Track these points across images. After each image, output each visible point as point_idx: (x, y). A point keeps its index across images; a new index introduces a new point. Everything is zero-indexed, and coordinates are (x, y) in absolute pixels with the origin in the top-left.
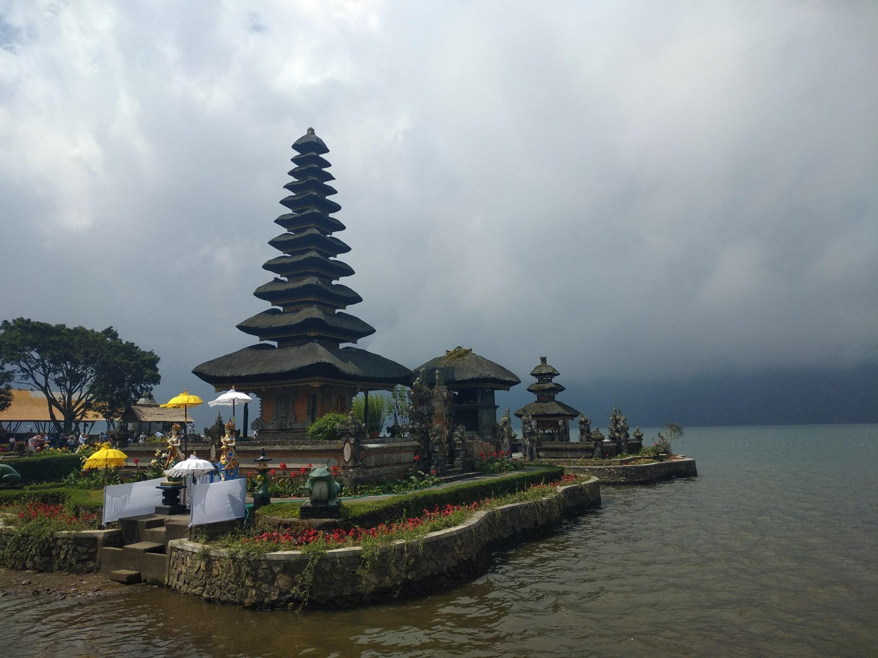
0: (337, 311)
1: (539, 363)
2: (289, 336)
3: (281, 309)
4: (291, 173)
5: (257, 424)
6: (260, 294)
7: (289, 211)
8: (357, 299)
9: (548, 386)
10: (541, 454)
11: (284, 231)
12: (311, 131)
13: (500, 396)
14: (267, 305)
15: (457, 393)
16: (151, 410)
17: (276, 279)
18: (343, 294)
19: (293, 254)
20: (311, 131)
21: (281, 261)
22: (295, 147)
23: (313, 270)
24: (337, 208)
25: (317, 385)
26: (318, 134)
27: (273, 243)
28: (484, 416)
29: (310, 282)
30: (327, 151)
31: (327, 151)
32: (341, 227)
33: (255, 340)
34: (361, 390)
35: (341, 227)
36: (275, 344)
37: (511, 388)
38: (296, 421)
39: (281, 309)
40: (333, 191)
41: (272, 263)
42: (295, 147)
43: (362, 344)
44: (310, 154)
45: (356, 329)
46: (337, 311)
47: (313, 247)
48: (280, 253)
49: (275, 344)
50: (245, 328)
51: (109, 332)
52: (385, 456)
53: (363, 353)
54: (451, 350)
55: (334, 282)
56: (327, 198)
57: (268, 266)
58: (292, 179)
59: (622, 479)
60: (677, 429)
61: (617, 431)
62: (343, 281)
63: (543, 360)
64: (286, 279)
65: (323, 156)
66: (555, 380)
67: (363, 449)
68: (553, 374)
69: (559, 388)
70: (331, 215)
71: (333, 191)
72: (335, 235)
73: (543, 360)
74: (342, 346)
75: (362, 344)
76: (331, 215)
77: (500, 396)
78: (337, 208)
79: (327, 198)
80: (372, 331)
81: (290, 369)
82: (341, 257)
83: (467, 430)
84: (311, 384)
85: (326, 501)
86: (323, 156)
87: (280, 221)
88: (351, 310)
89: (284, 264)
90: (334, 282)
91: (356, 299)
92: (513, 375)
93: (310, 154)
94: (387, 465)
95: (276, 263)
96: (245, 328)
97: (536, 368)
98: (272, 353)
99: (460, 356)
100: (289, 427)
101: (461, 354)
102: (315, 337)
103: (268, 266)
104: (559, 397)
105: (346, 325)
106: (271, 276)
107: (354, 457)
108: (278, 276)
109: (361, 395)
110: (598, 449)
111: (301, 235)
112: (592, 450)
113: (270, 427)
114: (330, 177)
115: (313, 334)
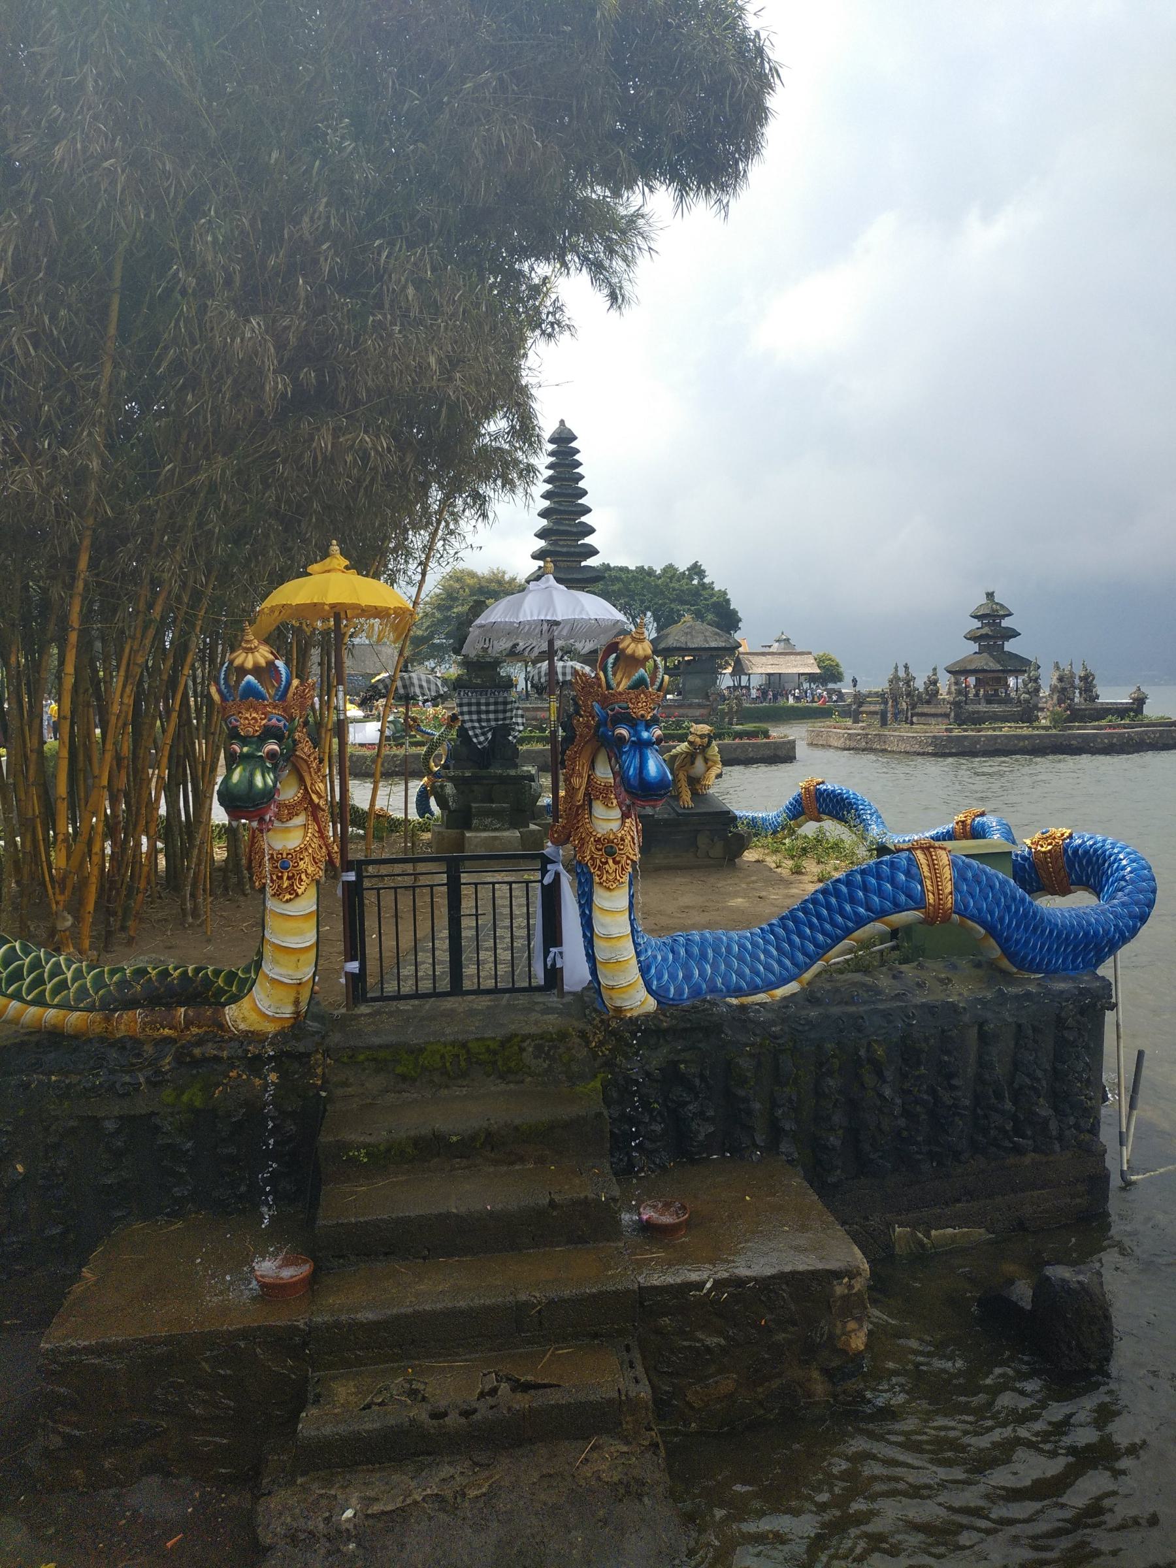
10: (915, 719)
12: (562, 422)
16: (763, 659)
20: (562, 422)
26: (568, 425)
30: (575, 438)
31: (575, 438)
51: (696, 570)
55: (583, 564)
59: (930, 749)
61: (1028, 693)
63: (990, 595)
69: (1013, 634)
70: (580, 501)
73: (990, 595)
76: (580, 501)
82: (588, 540)
86: (573, 445)
90: (583, 564)
104: (1010, 646)
110: (952, 714)
112: (947, 715)
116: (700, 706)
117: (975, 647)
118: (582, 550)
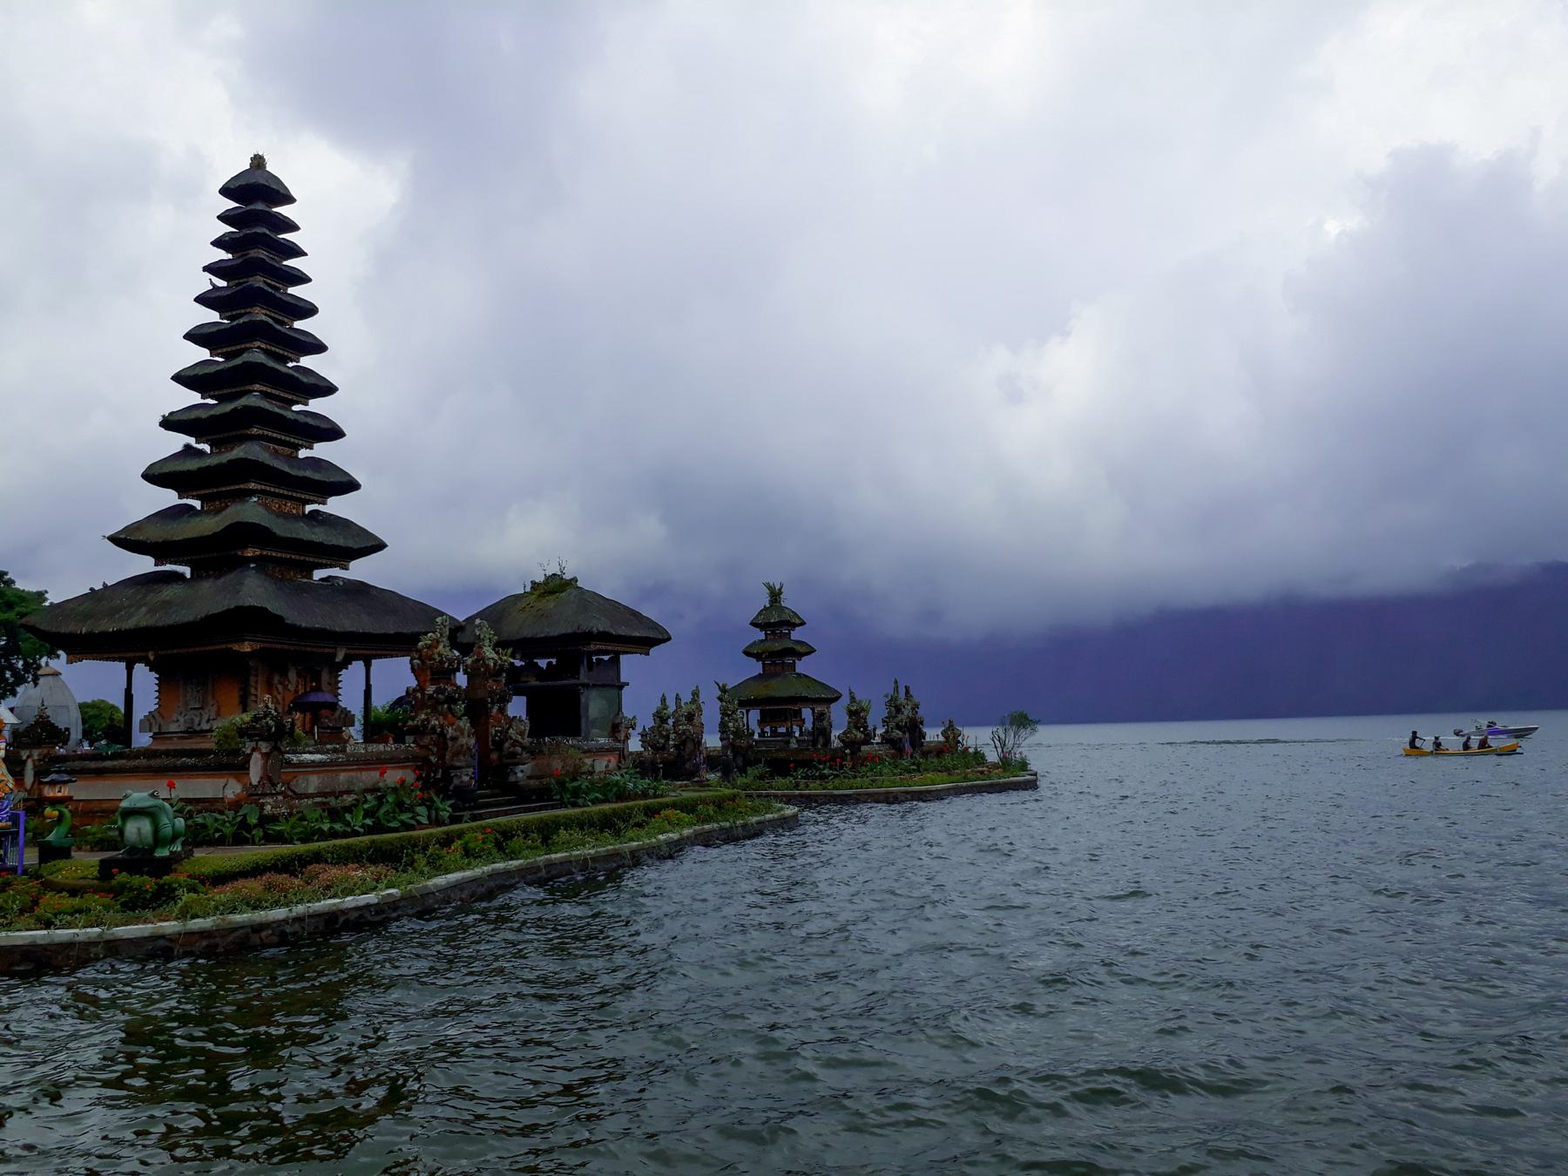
0: (308, 508)
1: (765, 601)
2: (213, 555)
3: (197, 504)
4: (217, 243)
5: (148, 722)
6: (156, 476)
7: (213, 316)
8: (348, 485)
9: (778, 646)
11: (203, 354)
12: (258, 162)
13: (631, 665)
14: (168, 498)
15: (554, 661)
17: (188, 447)
18: (317, 477)
19: (221, 399)
20: (258, 162)
21: (193, 415)
22: (226, 191)
23: (255, 431)
24: (309, 310)
25: (247, 648)
26: (270, 167)
27: (178, 378)
28: (594, 705)
29: (242, 455)
30: (288, 199)
31: (288, 199)
32: (318, 347)
33: (144, 564)
34: (357, 658)
35: (318, 347)
36: (187, 571)
37: (653, 651)
38: (218, 714)
39: (197, 504)
40: (302, 279)
41: (176, 418)
42: (226, 191)
43: (360, 570)
44: (256, 204)
45: (341, 542)
46: (308, 508)
47: (257, 387)
48: (195, 398)
49: (187, 571)
50: (126, 540)
52: (343, 777)
53: (360, 590)
54: (540, 579)
55: (303, 453)
56: (291, 290)
57: (169, 423)
58: (223, 255)
60: (1022, 721)
62: (321, 450)
63: (775, 595)
64: (206, 448)
65: (283, 210)
66: (796, 634)
67: (289, 763)
68: (792, 623)
70: (298, 325)
71: (302, 279)
72: (307, 361)
73: (775, 595)
74: (318, 574)
75: (360, 570)
76: (298, 325)
77: (631, 665)
78: (309, 310)
79: (291, 290)
80: (380, 546)
81: (191, 618)
82: (316, 405)
83: (575, 731)
84: (236, 647)
85: (152, 849)
86: (283, 210)
87: (196, 336)
88: (336, 506)
89: (198, 420)
90: (303, 453)
91: (348, 485)
92: (655, 626)
93: (256, 204)
94: (349, 792)
95: (184, 417)
96: (126, 540)
97: (760, 613)
98: (170, 592)
99: (552, 592)
100: (205, 727)
101: (555, 586)
102: (251, 559)
103: (169, 423)
104: (802, 666)
105: (318, 535)
106: (177, 441)
107: (268, 778)
108: (192, 441)
109: (357, 667)
111: (238, 361)
113: (173, 728)
114: (297, 252)
115: (249, 553)
116: (610, 750)
117: (756, 668)
118: (302, 419)
